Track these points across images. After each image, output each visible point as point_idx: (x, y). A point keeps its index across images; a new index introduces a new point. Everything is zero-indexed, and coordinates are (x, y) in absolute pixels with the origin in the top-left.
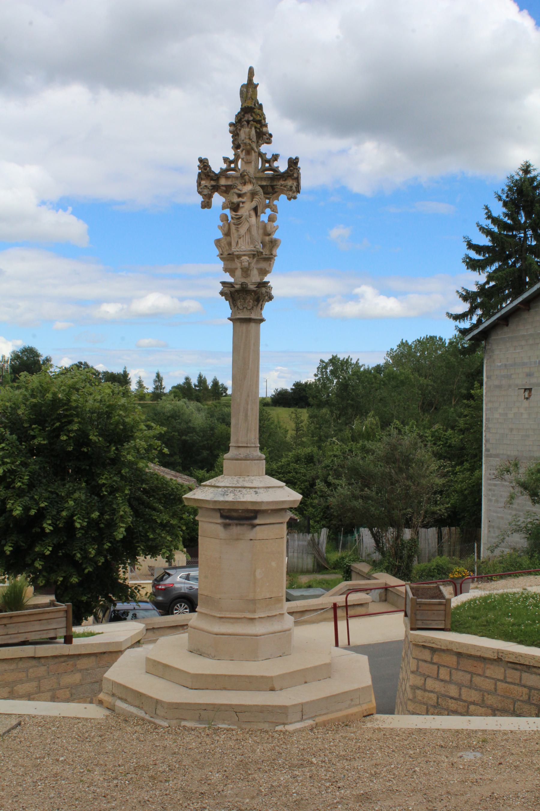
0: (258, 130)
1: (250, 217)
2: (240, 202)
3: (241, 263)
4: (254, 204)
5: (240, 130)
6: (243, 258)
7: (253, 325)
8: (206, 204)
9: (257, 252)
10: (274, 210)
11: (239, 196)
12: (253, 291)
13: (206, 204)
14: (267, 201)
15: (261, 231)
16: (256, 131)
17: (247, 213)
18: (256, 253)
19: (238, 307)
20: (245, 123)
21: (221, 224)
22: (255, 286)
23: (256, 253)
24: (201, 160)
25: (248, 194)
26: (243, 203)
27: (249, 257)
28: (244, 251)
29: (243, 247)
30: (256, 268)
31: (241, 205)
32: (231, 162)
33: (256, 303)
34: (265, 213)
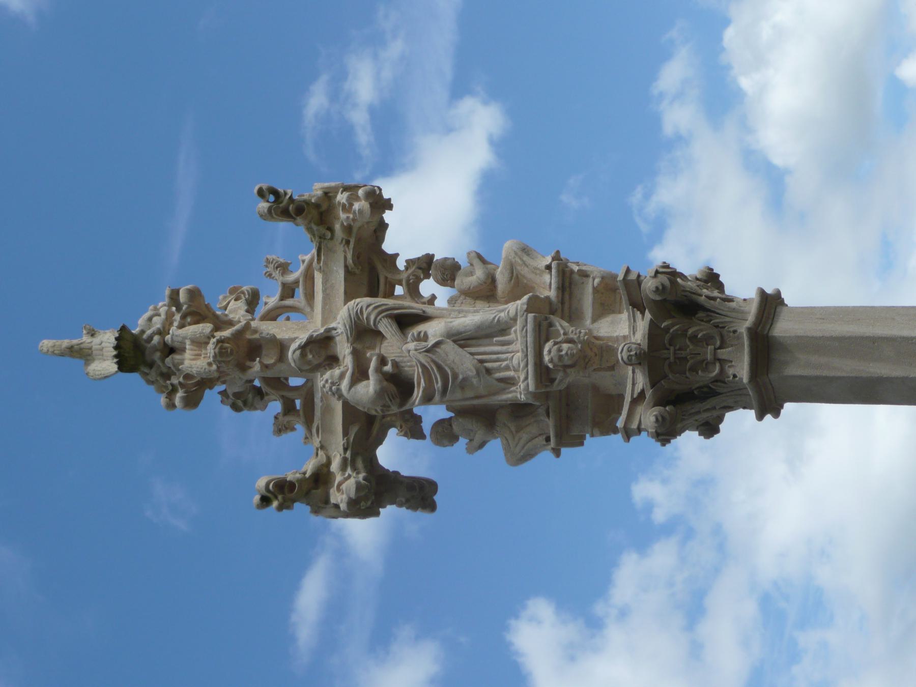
0: (189, 319)
1: (426, 338)
2: (378, 370)
3: (566, 367)
4: (387, 327)
5: (188, 376)
6: (546, 358)
7: (782, 328)
8: (419, 494)
9: (528, 311)
10: (425, 266)
11: (360, 374)
12: (653, 326)
13: (419, 494)
14: (399, 290)
15: (480, 304)
16: (190, 324)
17: (412, 346)
18: (531, 316)
19: (716, 380)
20: (168, 360)
21: (463, 442)
22: (638, 315)
23: (531, 316)
24: (265, 501)
25: (359, 346)
26: (383, 361)
27: (547, 340)
28: (527, 356)
29: (515, 362)
30: (595, 320)
31: (388, 368)
32: (289, 408)
33: (701, 314)
34: (433, 297)
